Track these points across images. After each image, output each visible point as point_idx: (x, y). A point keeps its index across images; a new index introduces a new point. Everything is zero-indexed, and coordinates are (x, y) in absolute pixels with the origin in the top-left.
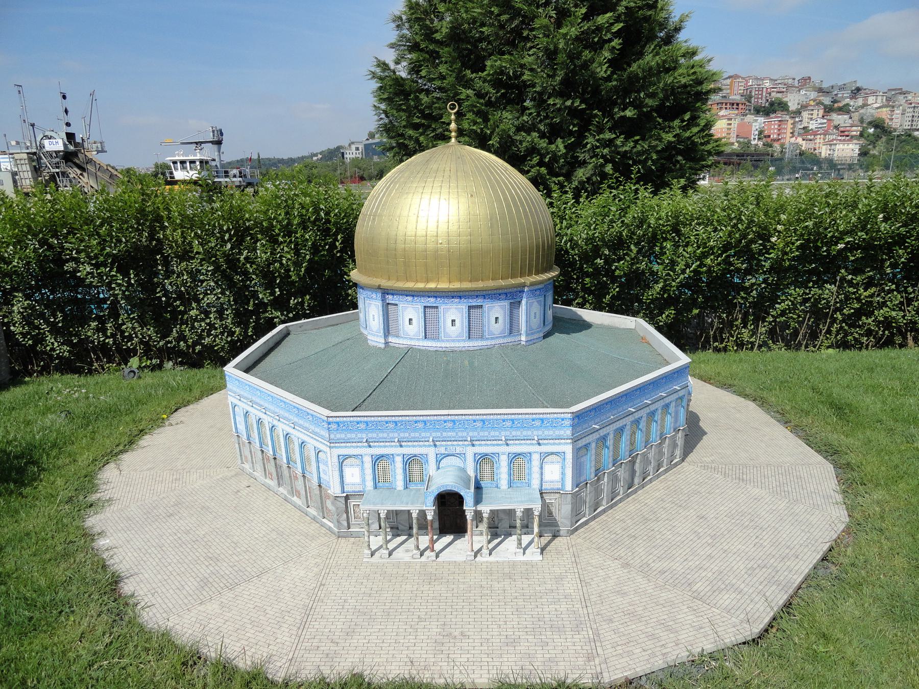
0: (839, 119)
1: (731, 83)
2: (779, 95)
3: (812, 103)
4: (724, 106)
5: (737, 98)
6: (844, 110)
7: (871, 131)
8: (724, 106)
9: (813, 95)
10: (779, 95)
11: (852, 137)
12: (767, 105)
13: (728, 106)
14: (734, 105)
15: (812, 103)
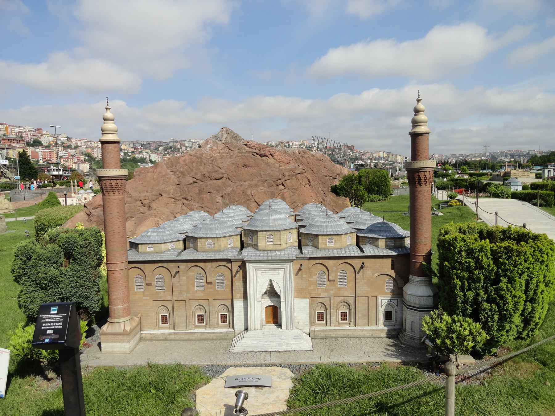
0: (72, 152)
1: (6, 128)
2: (35, 137)
3: (52, 142)
4: (12, 141)
5: (15, 136)
6: (69, 147)
7: (87, 158)
8: (12, 141)
9: (52, 139)
10: (35, 137)
11: (82, 160)
12: (31, 142)
13: (15, 141)
14: (18, 141)
15: (52, 142)
